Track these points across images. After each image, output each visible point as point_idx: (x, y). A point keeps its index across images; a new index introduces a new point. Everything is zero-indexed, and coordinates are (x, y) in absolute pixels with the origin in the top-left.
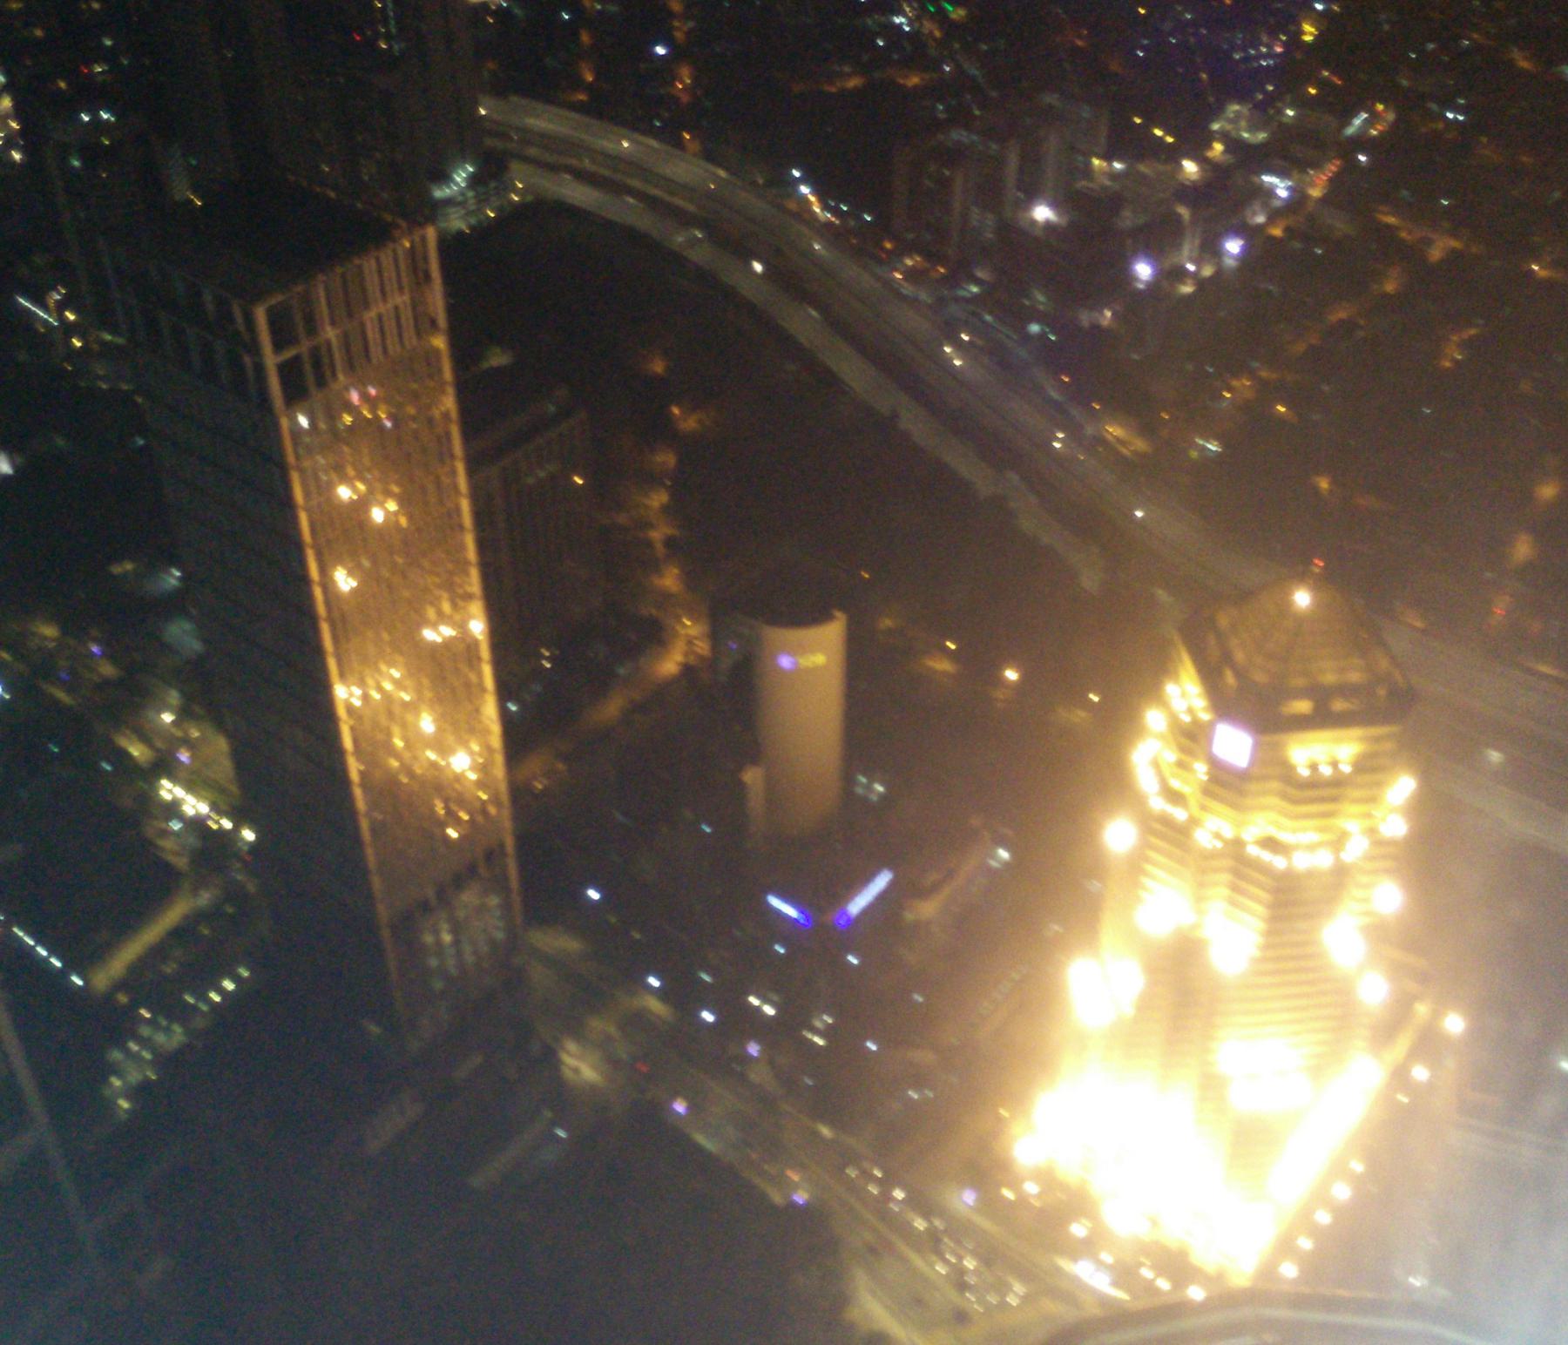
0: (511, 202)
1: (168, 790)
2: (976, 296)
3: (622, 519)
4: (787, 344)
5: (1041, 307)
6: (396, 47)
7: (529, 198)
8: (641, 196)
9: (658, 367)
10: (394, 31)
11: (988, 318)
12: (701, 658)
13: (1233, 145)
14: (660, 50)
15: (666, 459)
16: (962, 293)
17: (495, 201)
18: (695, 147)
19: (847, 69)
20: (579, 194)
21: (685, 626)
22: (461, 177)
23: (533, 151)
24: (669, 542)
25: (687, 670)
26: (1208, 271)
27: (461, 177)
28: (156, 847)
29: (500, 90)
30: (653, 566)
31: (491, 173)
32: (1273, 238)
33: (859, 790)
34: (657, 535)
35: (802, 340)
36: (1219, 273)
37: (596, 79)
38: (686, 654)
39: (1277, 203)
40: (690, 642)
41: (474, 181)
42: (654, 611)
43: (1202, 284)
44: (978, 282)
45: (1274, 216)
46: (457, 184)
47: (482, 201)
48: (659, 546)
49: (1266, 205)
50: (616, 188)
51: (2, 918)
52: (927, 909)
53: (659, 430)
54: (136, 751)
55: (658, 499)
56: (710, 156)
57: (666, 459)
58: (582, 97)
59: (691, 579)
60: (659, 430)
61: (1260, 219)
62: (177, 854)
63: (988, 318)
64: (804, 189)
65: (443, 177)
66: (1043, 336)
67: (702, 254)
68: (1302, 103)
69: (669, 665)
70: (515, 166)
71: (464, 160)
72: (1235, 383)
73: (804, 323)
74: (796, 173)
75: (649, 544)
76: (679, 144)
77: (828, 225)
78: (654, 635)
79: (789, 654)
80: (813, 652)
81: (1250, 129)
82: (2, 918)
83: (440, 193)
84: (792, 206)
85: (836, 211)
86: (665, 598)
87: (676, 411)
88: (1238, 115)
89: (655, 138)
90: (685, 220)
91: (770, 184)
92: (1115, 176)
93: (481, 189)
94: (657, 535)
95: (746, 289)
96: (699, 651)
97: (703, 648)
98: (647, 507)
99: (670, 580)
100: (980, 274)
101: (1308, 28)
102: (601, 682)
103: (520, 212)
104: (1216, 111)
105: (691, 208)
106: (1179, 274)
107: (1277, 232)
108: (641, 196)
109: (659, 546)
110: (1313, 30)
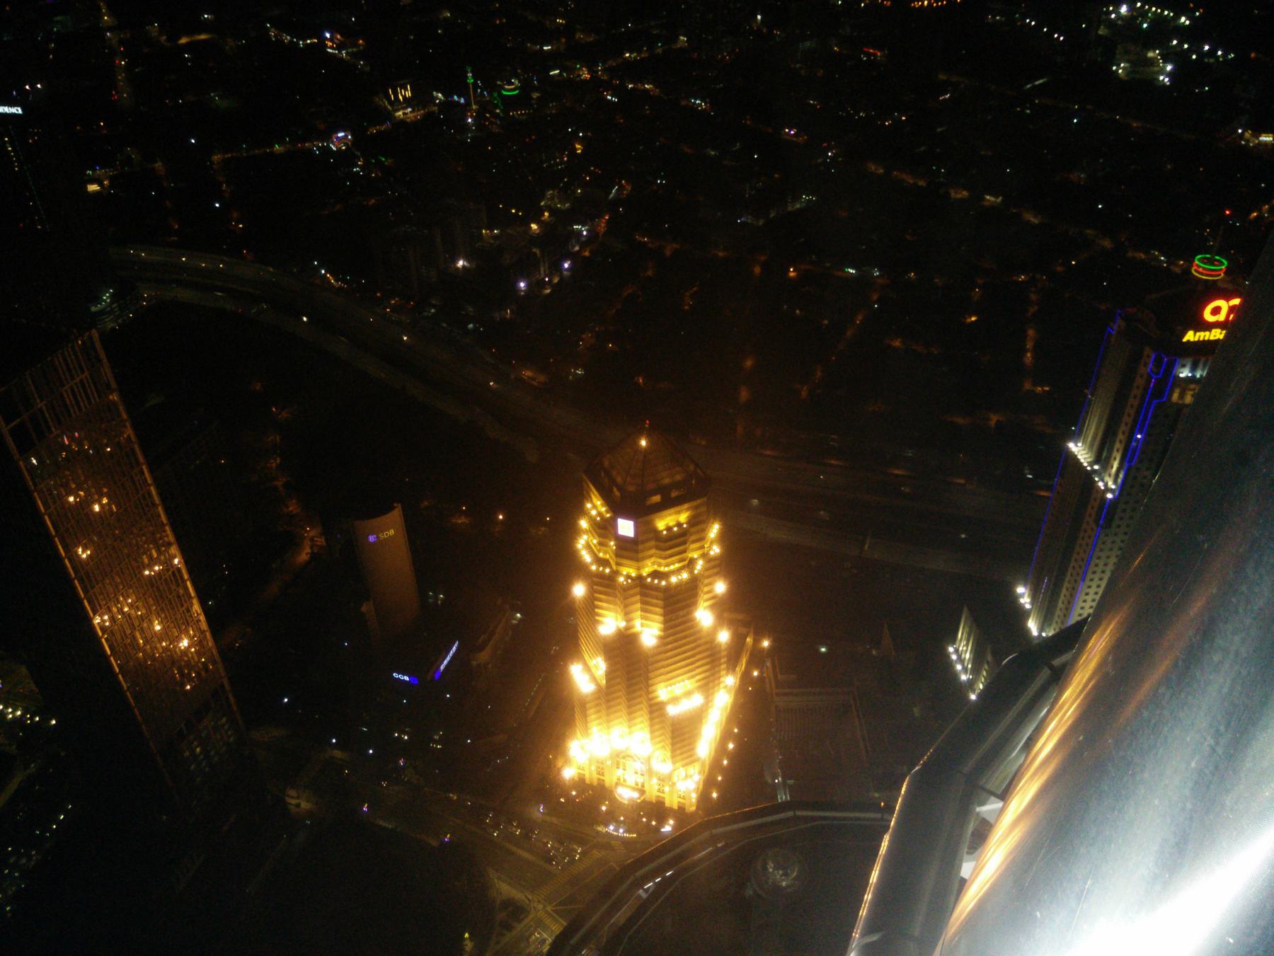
2: (434, 314)
5: (471, 314)
11: (444, 325)
13: (553, 212)
16: (425, 314)
20: (185, 295)
21: (307, 531)
25: (314, 557)
26: (556, 280)
32: (585, 257)
33: (431, 600)
34: (279, 484)
36: (561, 280)
38: (311, 548)
39: (584, 239)
40: (312, 539)
43: (556, 288)
44: (434, 306)
45: (583, 245)
46: (105, 301)
49: (578, 241)
52: (484, 656)
55: (275, 462)
61: (577, 248)
63: (444, 325)
65: (98, 300)
66: (475, 330)
68: (584, 185)
69: (304, 556)
72: (584, 336)
77: (341, 289)
78: (291, 541)
81: (560, 203)
88: (552, 198)
92: (496, 237)
93: (122, 302)
96: (318, 543)
97: (321, 541)
99: (293, 507)
100: (434, 302)
101: (578, 146)
104: (542, 197)
106: (542, 284)
107: (587, 254)
110: (579, 147)
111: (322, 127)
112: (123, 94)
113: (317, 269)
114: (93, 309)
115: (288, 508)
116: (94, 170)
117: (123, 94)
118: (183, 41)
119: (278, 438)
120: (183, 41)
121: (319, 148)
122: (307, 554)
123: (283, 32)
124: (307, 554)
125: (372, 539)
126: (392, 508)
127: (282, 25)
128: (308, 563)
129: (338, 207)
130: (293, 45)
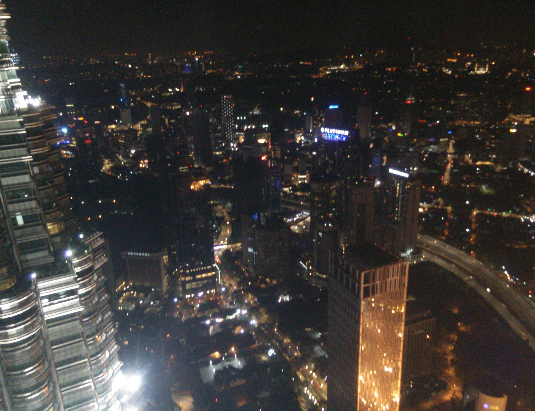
0: (420, 260)
1: (306, 390)
3: (439, 350)
4: (496, 314)
6: (399, 219)
7: (426, 260)
8: (457, 266)
9: (456, 311)
10: (399, 215)
12: (457, 398)
14: (468, 230)
15: (454, 337)
17: (417, 260)
18: (474, 255)
19: (522, 243)
20: (439, 261)
22: (409, 252)
23: (429, 249)
24: (452, 361)
25: (452, 400)
27: (409, 252)
28: (300, 404)
29: (422, 233)
30: (446, 366)
31: (417, 252)
34: (449, 358)
35: (501, 313)
37: (449, 234)
38: (453, 395)
40: (454, 392)
41: (412, 253)
42: (445, 379)
47: (413, 259)
48: (449, 361)
50: (449, 262)
51: (260, 410)
53: (453, 328)
54: (301, 377)
55: (451, 348)
56: (478, 258)
57: (454, 337)
58: (444, 238)
59: (458, 373)
60: (453, 328)
62: (305, 408)
64: (506, 272)
65: (404, 251)
67: (473, 284)
69: (448, 397)
70: (423, 252)
71: (410, 248)
73: (501, 308)
74: (504, 267)
75: (446, 359)
76: (470, 254)
77: (512, 283)
78: (444, 387)
79: (487, 403)
80: (496, 406)
82: (260, 410)
83: (403, 255)
84: (501, 276)
85: (515, 280)
86: (449, 377)
87: (459, 324)
89: (463, 251)
90: (469, 274)
91: (496, 269)
93: (413, 256)
94: (449, 358)
95: (484, 296)
96: (457, 395)
97: (459, 395)
98: (447, 349)
99: (451, 372)
102: (426, 396)
103: (423, 263)
105: (471, 271)
108: (457, 266)
109: (449, 361)
111: (529, 210)
112: (446, 179)
113: (504, 270)
114: (403, 255)
115: (448, 370)
116: (423, 203)
117: (446, 179)
118: (479, 163)
119: (456, 338)
120: (479, 163)
121: (524, 219)
122: (450, 397)
123: (526, 167)
124: (450, 397)
125: (486, 406)
126: (503, 397)
127: (525, 164)
128: (448, 402)
129: (524, 246)
130: (528, 174)
